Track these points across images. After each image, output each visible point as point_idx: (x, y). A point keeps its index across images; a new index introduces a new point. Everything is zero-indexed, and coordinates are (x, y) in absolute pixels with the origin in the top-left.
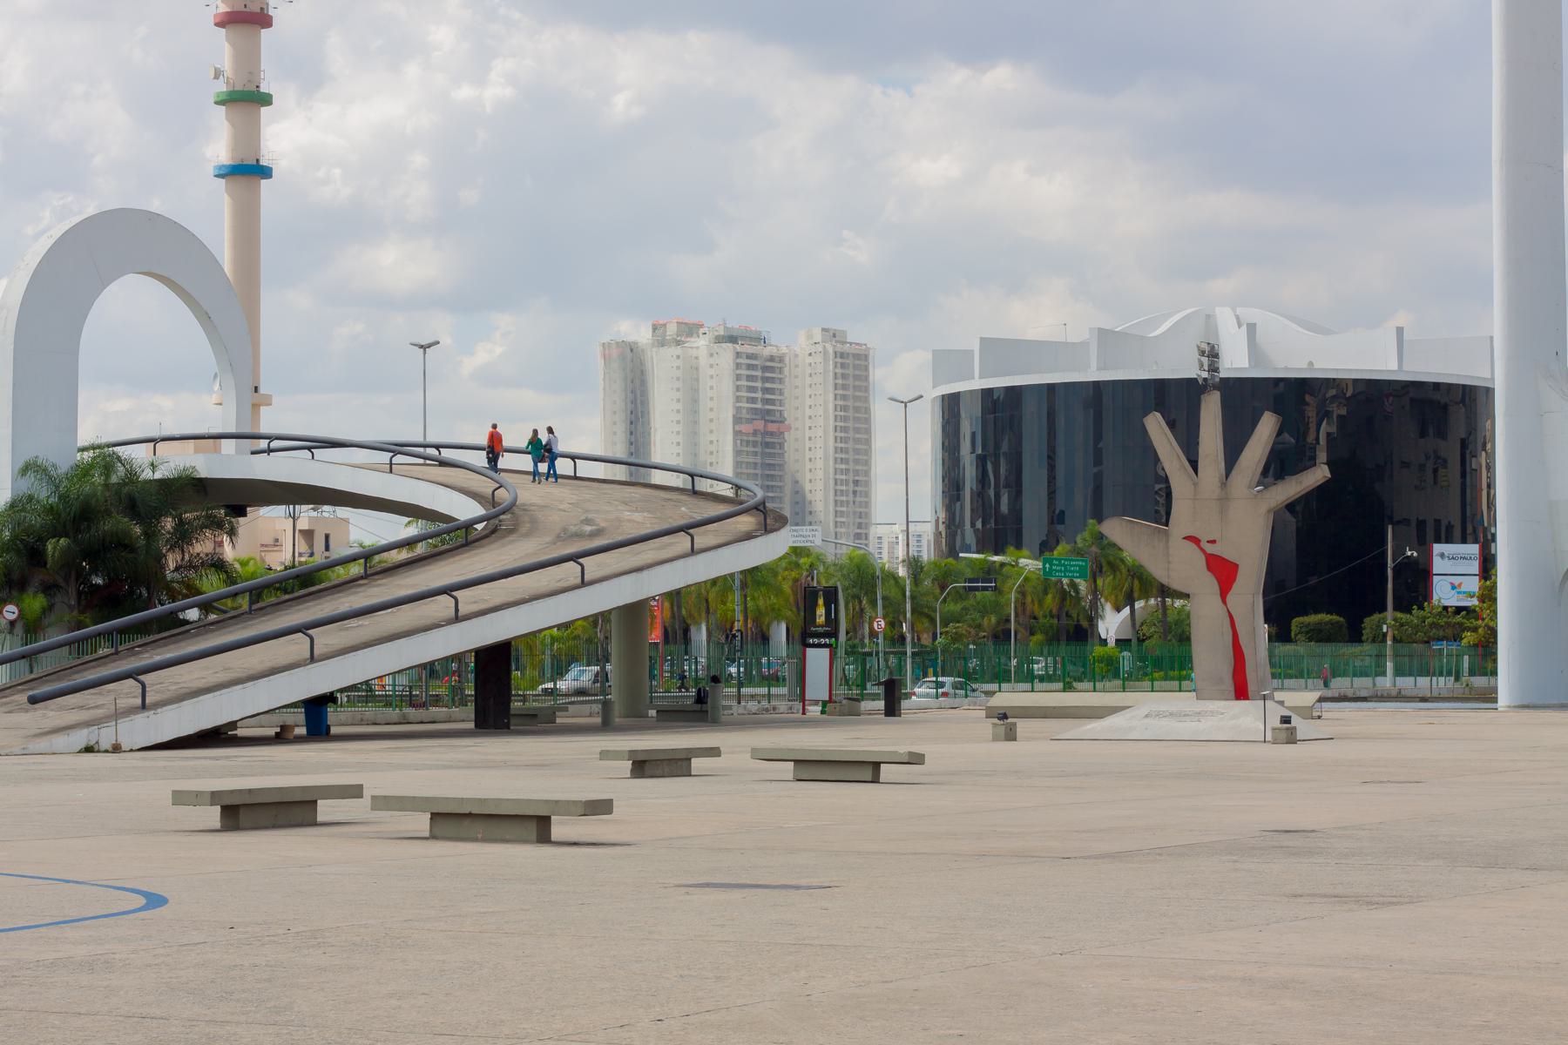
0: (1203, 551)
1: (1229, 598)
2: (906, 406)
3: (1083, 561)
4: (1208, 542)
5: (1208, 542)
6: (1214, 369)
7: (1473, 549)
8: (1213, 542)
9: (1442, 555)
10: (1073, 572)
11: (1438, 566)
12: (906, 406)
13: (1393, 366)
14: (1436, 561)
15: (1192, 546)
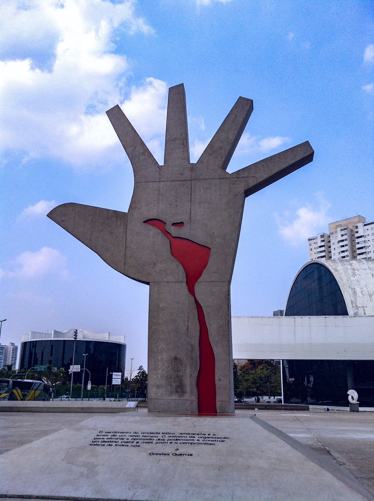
0: (167, 233)
1: (199, 287)
2: (1, 322)
3: (45, 366)
4: (173, 224)
5: (173, 224)
6: (75, 338)
7: (120, 374)
8: (180, 224)
9: (114, 375)
10: (43, 369)
11: (114, 377)
12: (1, 322)
13: (107, 339)
14: (113, 375)
15: (153, 231)
